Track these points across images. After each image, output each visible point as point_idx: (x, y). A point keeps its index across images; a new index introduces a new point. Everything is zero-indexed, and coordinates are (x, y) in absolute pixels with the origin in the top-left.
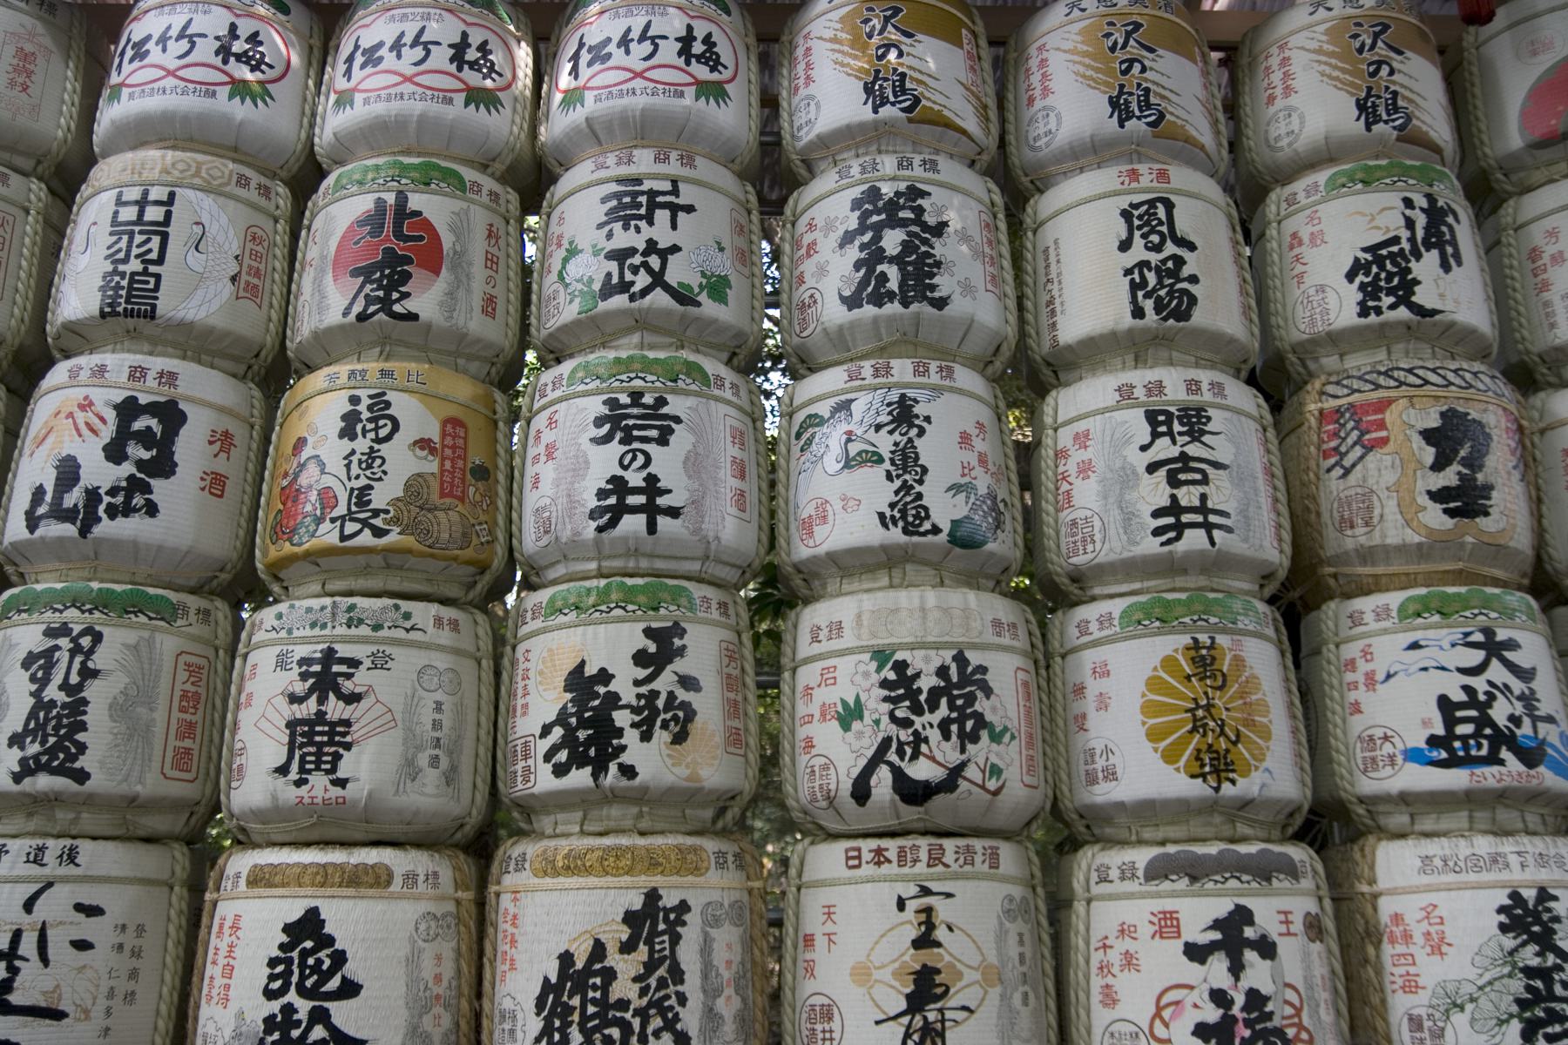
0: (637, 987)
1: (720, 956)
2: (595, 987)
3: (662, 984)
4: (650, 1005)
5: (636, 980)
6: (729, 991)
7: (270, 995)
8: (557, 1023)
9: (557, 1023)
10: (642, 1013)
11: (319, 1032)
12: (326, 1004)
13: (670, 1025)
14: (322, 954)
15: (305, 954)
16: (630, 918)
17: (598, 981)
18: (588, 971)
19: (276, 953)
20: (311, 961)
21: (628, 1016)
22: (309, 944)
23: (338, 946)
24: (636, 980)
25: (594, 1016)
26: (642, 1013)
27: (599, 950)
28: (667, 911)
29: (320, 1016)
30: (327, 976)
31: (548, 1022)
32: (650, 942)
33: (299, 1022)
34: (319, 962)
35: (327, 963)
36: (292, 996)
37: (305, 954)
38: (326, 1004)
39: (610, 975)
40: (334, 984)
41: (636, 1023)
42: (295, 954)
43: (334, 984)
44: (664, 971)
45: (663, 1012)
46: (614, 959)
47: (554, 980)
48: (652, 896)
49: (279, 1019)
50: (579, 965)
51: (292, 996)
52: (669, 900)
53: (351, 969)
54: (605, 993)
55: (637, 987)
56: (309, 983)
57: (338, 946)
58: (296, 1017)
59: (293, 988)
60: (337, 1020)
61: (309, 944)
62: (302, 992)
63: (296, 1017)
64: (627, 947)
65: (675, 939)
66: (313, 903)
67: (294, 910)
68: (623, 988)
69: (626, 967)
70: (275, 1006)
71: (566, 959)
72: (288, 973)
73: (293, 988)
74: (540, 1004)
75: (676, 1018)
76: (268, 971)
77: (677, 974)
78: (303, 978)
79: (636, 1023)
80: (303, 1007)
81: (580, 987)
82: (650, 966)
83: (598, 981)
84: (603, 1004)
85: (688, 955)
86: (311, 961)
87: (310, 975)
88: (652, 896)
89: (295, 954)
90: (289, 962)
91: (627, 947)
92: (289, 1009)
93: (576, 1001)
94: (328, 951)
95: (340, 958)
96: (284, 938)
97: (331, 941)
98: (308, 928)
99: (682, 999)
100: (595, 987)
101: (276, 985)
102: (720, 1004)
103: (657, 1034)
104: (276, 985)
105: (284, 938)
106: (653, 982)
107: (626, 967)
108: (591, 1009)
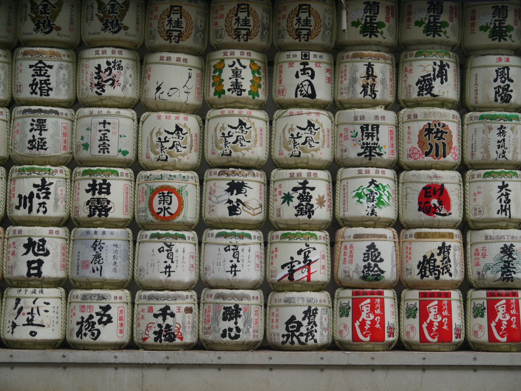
0: (441, 263)
1: (457, 257)
2: (432, 263)
3: (446, 262)
4: (444, 267)
5: (441, 261)
6: (459, 265)
7: (364, 261)
8: (423, 270)
9: (423, 270)
10: (442, 268)
11: (376, 269)
13: (448, 271)
16: (439, 248)
17: (433, 261)
18: (430, 259)
20: (373, 254)
21: (439, 269)
22: (373, 250)
23: (379, 251)
24: (441, 261)
25: (432, 269)
26: (442, 268)
27: (432, 255)
28: (447, 247)
29: (376, 266)
30: (377, 257)
31: (421, 270)
32: (443, 253)
33: (372, 267)
34: (375, 254)
35: (377, 254)
36: (370, 261)
37: (372, 252)
39: (435, 260)
40: (378, 259)
41: (441, 270)
42: (370, 252)
43: (378, 259)
44: (446, 260)
45: (447, 268)
46: (436, 257)
47: (422, 261)
48: (444, 244)
50: (428, 258)
51: (370, 261)
52: (447, 244)
53: (382, 256)
54: (434, 264)
55: (441, 263)
57: (379, 251)
60: (379, 266)
61: (373, 250)
62: (372, 260)
64: (439, 254)
65: (449, 253)
67: (369, 243)
68: (438, 263)
69: (439, 258)
70: (366, 263)
71: (425, 257)
72: (368, 257)
74: (418, 266)
75: (449, 270)
77: (449, 261)
79: (441, 270)
80: (373, 264)
81: (428, 262)
82: (444, 258)
83: (433, 261)
84: (434, 266)
85: (451, 256)
86: (373, 254)
88: (444, 244)
89: (370, 252)
90: (369, 254)
91: (439, 254)
92: (369, 264)
93: (428, 266)
95: (379, 254)
96: (367, 249)
97: (377, 250)
98: (372, 247)
99: (450, 266)
100: (432, 263)
101: (366, 259)
102: (457, 267)
103: (446, 273)
104: (366, 259)
105: (367, 249)
106: (444, 262)
107: (439, 258)
108: (431, 267)
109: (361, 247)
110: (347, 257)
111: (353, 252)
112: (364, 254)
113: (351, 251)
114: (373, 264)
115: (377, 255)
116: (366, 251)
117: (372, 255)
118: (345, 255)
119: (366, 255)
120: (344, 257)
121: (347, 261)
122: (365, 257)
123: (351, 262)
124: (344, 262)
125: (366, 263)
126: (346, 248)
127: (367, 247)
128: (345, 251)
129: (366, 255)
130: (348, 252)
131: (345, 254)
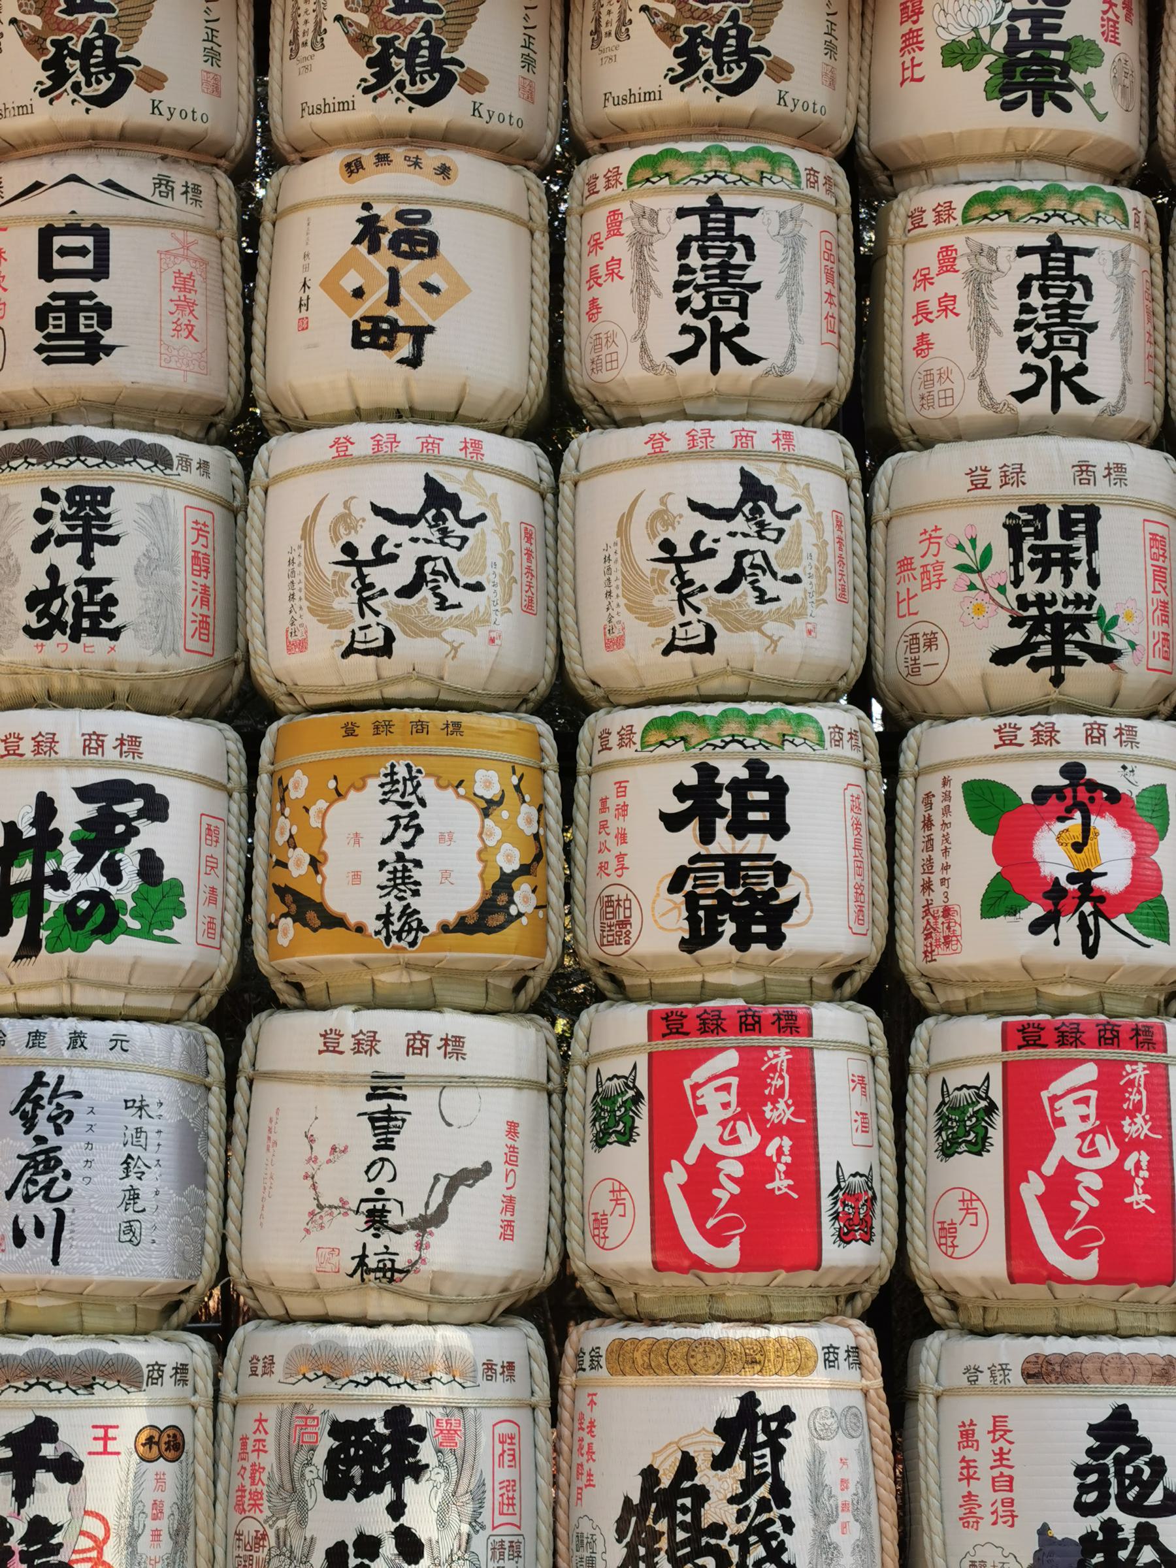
7: (1083, 1509)
11: (1148, 1554)
12: (1152, 1521)
14: (1141, 1461)
15: (1121, 1461)
19: (1084, 1459)
20: (1129, 1470)
22: (1123, 1449)
23: (1156, 1452)
29: (1147, 1535)
30: (1148, 1488)
33: (1124, 1543)
34: (1139, 1471)
35: (1147, 1472)
36: (1113, 1511)
37: (1121, 1461)
38: (1152, 1521)
40: (1156, 1497)
43: (1156, 1497)
49: (1100, 1537)
51: (1113, 1511)
56: (1131, 1495)
57: (1156, 1452)
58: (1121, 1536)
59: (1113, 1501)
61: (1123, 1449)
62: (1125, 1506)
63: (1121, 1536)
66: (1121, 1402)
67: (1101, 1411)
70: (1093, 1523)
72: (1102, 1486)
73: (1113, 1501)
76: (1078, 1481)
78: (1123, 1490)
80: (1129, 1524)
86: (1129, 1470)
87: (1131, 1487)
90: (1103, 1471)
92: (1111, 1527)
94: (1146, 1458)
95: (1158, 1466)
96: (1091, 1442)
97: (1144, 1446)
98: (1118, 1429)
101: (1091, 1497)
104: (1091, 1497)
105: (1091, 1442)
109: (1060, 1428)
110: (982, 1488)
111: (1013, 1458)
112: (1081, 1472)
113: (1001, 1455)
114: (1129, 1524)
115: (1147, 1472)
116: (1090, 1452)
117: (1120, 1474)
118: (969, 1478)
119: (1093, 1478)
120: (963, 1489)
121: (984, 1512)
122: (1083, 1489)
123: (1009, 1514)
124: (970, 1518)
125: (1093, 1523)
126: (967, 1435)
127: (1093, 1430)
128: (969, 1454)
129: (1093, 1478)
130: (984, 1457)
131: (968, 1471)
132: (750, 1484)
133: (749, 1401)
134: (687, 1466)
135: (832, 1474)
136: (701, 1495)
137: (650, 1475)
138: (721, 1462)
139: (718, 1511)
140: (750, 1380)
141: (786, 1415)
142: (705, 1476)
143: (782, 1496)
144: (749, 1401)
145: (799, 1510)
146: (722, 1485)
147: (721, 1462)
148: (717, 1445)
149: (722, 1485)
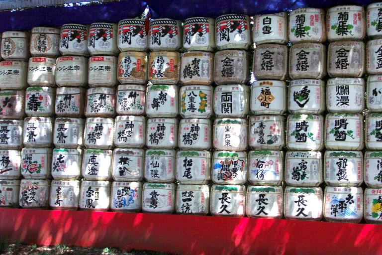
132: (195, 67)
133: (195, 59)
134: (189, 65)
135: (204, 66)
136: (190, 68)
137: (186, 66)
138: (192, 65)
139: (192, 69)
140: (196, 57)
141: (199, 60)
142: (191, 66)
143: (198, 68)
144: (195, 59)
145: (200, 69)
146: (192, 67)
147: (192, 65)
148: (192, 63)
149: (192, 67)
